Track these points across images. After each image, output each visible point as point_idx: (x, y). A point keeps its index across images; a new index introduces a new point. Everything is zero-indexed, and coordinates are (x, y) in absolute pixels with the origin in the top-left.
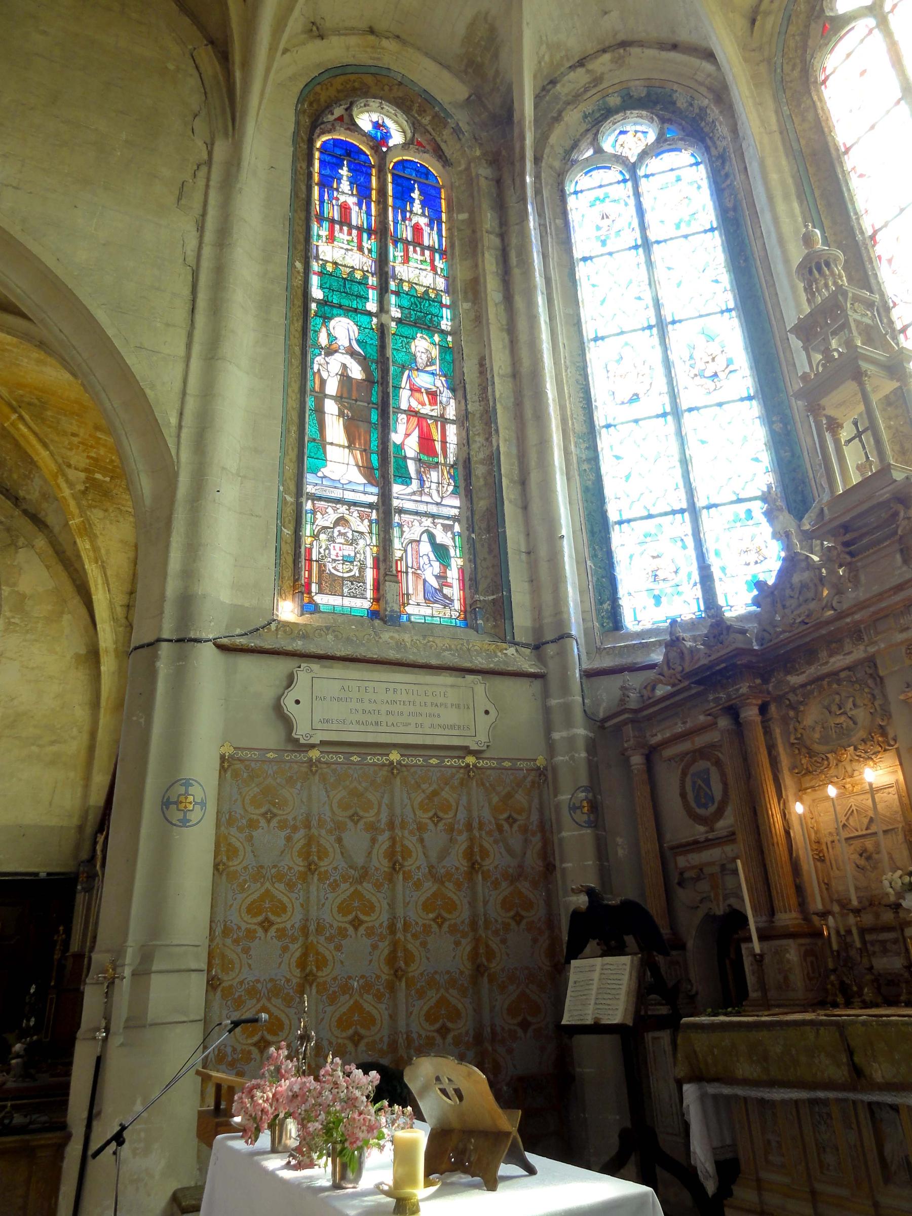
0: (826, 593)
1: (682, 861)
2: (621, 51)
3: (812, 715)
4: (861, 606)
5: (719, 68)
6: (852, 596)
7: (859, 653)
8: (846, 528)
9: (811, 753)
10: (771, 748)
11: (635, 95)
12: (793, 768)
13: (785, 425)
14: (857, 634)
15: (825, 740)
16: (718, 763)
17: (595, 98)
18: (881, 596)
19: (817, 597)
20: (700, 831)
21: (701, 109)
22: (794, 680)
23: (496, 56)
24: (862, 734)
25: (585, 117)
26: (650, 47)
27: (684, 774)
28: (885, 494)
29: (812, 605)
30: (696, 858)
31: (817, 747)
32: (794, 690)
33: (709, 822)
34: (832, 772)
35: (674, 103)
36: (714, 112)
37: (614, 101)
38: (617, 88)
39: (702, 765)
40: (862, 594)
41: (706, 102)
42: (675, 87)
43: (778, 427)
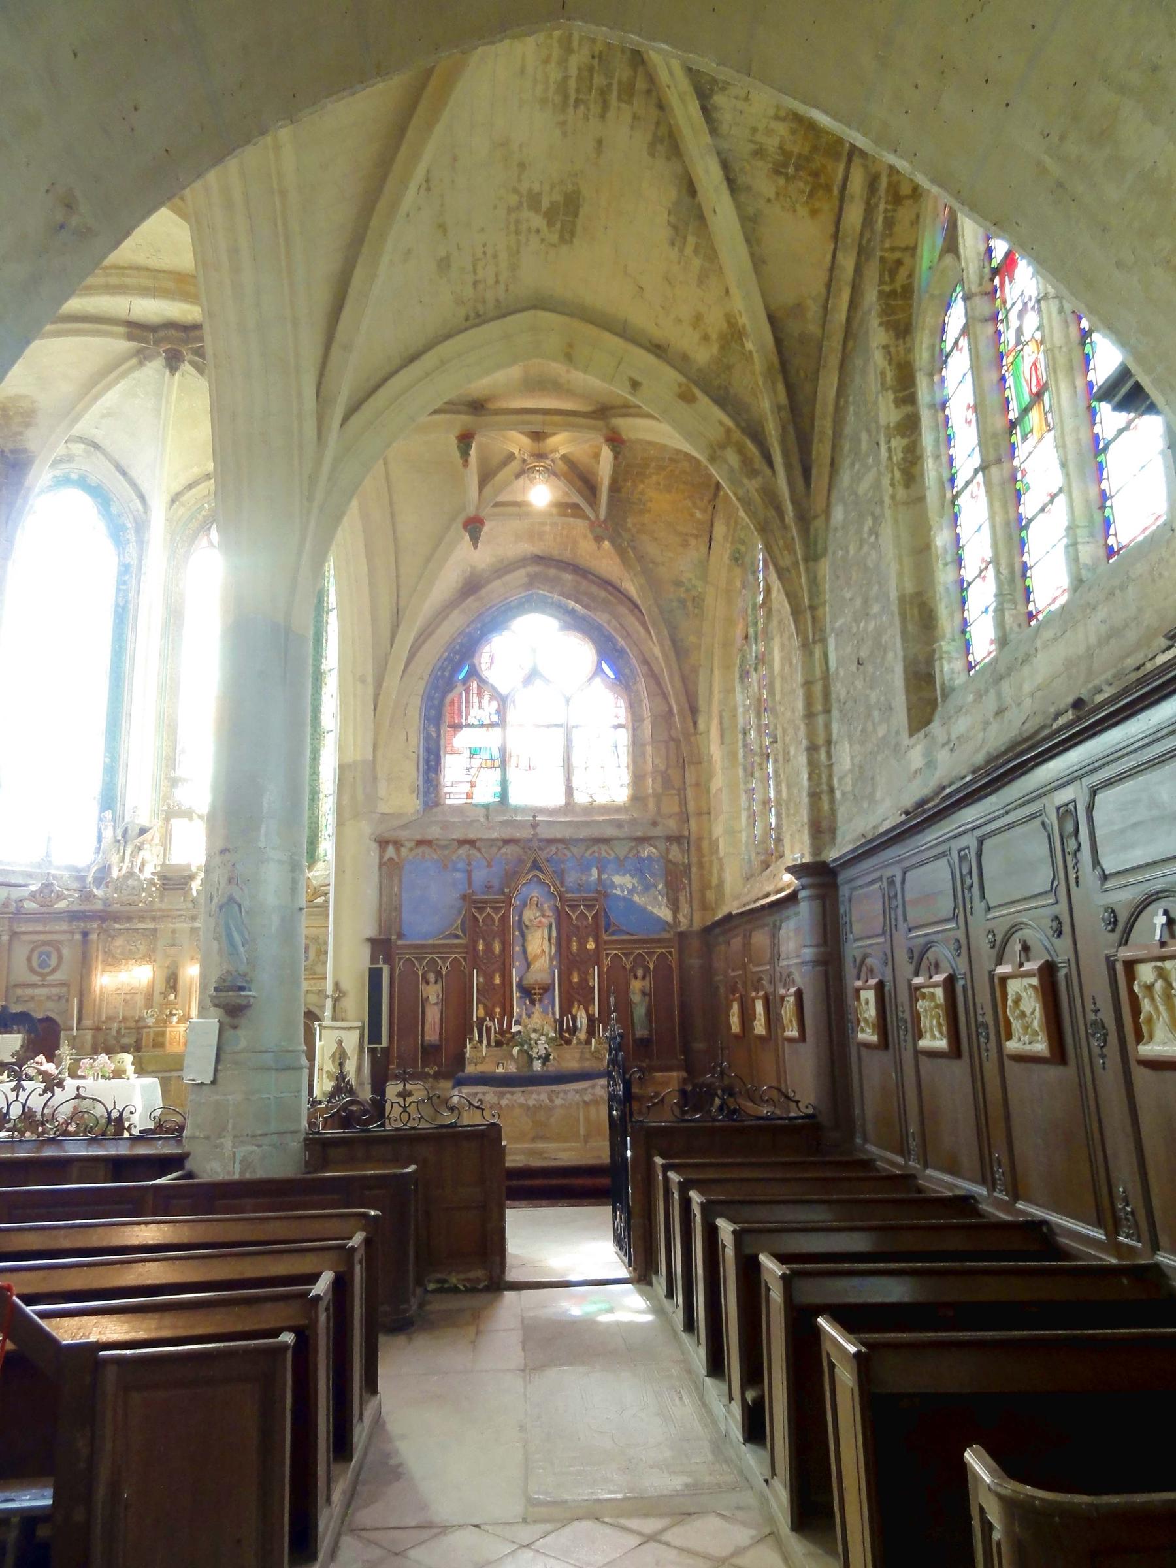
0: (144, 894)
1: (19, 992)
2: (93, 449)
3: (119, 942)
4: (161, 910)
5: (146, 512)
6: (158, 905)
7: (151, 926)
8: (165, 878)
9: (114, 957)
10: (98, 950)
11: (88, 480)
12: (103, 962)
13: (112, 761)
14: (154, 919)
15: (122, 953)
16: (59, 951)
17: (67, 471)
18: (171, 910)
19: (139, 895)
20: (35, 979)
21: (124, 525)
22: (117, 926)
23: (28, 425)
24: (141, 955)
25: (55, 477)
26: (110, 461)
27: (32, 950)
28: (186, 874)
29: (135, 898)
30: (29, 991)
31: (117, 956)
32: (114, 930)
33: (43, 976)
34: (122, 967)
35: (110, 506)
36: (132, 536)
37: (74, 476)
38: (82, 472)
39: (48, 948)
40: (163, 906)
41: (129, 525)
42: (115, 499)
43: (108, 760)
